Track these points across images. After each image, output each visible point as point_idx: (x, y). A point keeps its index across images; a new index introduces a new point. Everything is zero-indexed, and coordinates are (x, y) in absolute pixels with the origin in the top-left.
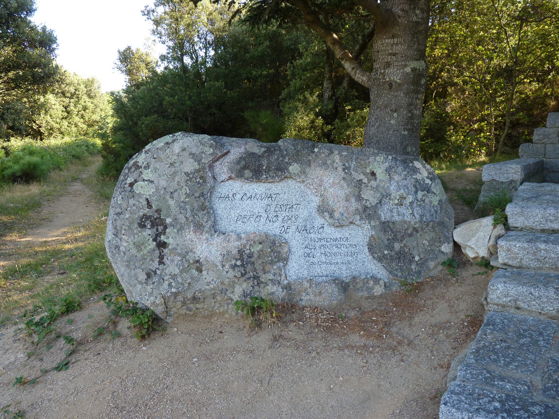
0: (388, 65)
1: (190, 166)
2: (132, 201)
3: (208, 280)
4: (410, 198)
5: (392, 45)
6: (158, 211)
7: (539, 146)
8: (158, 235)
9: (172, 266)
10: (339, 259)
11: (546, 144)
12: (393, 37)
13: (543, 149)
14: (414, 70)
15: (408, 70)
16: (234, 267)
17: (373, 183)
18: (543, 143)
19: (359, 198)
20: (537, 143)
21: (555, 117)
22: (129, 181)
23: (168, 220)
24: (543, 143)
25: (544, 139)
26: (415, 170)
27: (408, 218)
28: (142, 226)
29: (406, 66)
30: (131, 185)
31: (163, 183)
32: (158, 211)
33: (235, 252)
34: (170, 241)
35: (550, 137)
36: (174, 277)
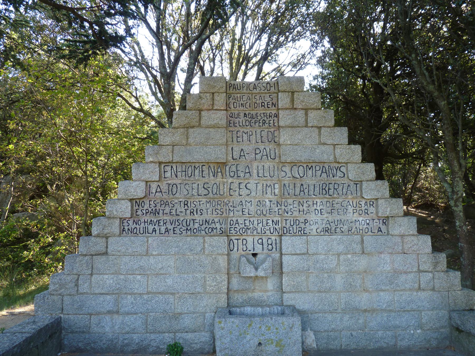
7: (55, 298)
11: (63, 296)
13: (60, 302)
18: (60, 295)
20: (53, 295)
21: (73, 261)
24: (60, 295)
25: (60, 289)
35: (67, 286)
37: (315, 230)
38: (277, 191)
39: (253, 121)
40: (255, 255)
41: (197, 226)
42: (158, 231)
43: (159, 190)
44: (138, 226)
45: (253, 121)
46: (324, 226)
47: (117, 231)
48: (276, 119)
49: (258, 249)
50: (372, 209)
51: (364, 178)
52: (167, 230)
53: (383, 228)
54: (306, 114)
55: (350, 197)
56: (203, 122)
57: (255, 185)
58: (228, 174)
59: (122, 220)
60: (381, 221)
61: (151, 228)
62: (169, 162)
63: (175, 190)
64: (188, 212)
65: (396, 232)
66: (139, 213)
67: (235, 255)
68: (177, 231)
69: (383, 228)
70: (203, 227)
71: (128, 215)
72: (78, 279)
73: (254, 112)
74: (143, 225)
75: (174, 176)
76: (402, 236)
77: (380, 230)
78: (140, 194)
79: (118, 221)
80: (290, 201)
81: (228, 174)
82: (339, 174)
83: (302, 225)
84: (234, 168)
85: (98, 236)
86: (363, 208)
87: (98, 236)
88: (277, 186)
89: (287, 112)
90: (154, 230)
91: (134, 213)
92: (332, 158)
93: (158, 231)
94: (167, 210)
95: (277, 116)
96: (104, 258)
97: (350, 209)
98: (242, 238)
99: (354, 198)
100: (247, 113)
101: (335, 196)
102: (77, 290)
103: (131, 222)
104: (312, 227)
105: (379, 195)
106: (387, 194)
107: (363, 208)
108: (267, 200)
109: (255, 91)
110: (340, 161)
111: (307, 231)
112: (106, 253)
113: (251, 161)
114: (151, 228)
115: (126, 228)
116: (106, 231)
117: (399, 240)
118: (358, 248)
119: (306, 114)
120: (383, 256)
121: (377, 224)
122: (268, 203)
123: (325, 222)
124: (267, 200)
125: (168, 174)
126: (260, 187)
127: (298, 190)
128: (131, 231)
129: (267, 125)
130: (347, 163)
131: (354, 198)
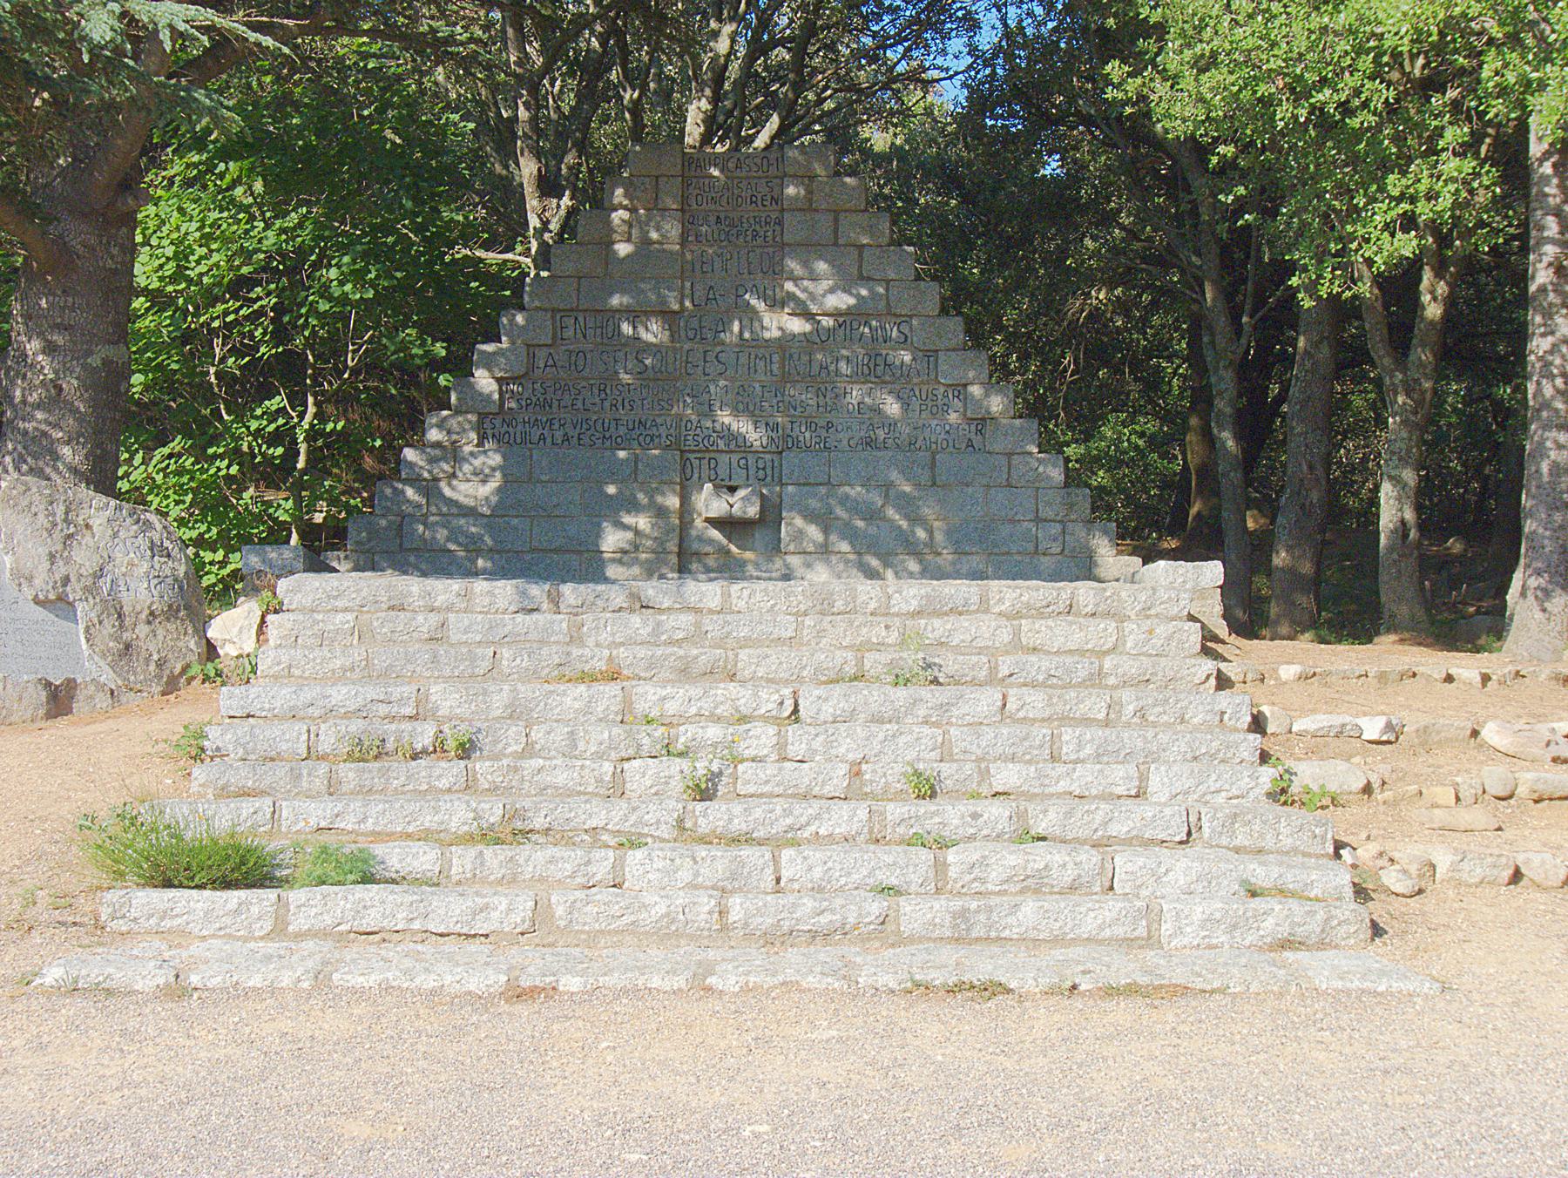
4: (146, 566)
5: (63, 309)
14: (106, 362)
15: (95, 361)
25: (369, 540)
26: (148, 525)
29: (89, 353)
37: (845, 442)
38: (775, 367)
39: (734, 231)
41: (622, 430)
42: (549, 440)
43: (550, 362)
44: (511, 430)
45: (734, 231)
46: (862, 433)
48: (778, 228)
51: (940, 345)
52: (566, 438)
53: (977, 440)
54: (836, 220)
55: (915, 380)
57: (733, 356)
58: (683, 333)
60: (973, 427)
61: (536, 433)
62: (572, 310)
63: (581, 363)
64: (607, 404)
65: (997, 448)
68: (586, 440)
70: (635, 434)
72: (401, 525)
73: (736, 215)
74: (520, 427)
75: (579, 335)
76: (1010, 455)
77: (970, 444)
81: (683, 333)
83: (824, 434)
84: (695, 323)
86: (940, 402)
88: (776, 358)
89: (799, 216)
90: (543, 438)
93: (549, 440)
94: (567, 400)
95: (780, 223)
98: (707, 456)
99: (923, 382)
100: (722, 216)
101: (887, 378)
102: (401, 545)
103: (498, 422)
104: (841, 436)
107: (940, 402)
108: (757, 385)
109: (738, 173)
110: (898, 311)
111: (831, 443)
113: (727, 312)
114: (536, 433)
115: (489, 432)
117: (1003, 461)
119: (836, 220)
120: (970, 490)
122: (758, 388)
123: (864, 427)
124: (757, 385)
125: (569, 333)
126: (743, 360)
129: (760, 241)
130: (911, 317)
131: (923, 382)
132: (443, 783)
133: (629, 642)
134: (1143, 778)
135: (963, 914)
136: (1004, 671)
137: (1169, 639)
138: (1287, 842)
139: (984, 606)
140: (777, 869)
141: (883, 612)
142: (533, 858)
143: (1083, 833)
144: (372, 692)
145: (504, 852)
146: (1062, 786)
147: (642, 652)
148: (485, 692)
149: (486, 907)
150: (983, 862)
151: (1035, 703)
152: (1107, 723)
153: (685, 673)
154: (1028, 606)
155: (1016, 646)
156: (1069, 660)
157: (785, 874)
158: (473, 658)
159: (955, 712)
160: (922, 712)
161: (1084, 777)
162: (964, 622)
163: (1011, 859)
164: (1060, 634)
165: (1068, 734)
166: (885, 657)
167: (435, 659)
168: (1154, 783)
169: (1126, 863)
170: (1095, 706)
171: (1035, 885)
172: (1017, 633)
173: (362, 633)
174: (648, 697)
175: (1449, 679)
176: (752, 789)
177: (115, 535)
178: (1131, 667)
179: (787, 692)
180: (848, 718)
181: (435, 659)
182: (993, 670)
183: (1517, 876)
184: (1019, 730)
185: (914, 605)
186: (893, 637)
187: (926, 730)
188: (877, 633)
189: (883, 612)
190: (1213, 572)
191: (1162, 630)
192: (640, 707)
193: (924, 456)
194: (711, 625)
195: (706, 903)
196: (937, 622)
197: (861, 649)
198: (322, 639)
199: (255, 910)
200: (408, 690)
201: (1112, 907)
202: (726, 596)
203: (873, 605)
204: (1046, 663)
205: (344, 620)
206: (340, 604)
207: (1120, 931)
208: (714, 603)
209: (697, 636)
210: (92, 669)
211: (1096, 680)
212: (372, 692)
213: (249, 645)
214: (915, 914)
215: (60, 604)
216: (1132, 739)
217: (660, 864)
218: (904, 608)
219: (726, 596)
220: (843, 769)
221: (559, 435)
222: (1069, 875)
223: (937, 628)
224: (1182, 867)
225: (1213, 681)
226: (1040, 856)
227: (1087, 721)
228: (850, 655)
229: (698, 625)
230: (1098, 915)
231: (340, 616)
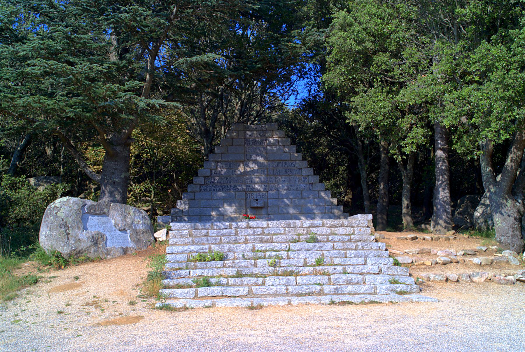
0: (113, 173)
1: (76, 207)
2: (57, 219)
3: (83, 246)
4: (141, 222)
6: (66, 222)
8: (66, 230)
9: (72, 242)
10: (121, 241)
12: (116, 161)
14: (125, 177)
15: (123, 176)
16: (91, 241)
17: (129, 216)
19: (126, 221)
22: (54, 212)
23: (70, 225)
26: (142, 213)
27: (141, 228)
28: (61, 228)
29: (121, 174)
30: (56, 213)
31: (67, 213)
32: (66, 222)
33: (91, 237)
34: (71, 232)
36: (73, 244)
38: (266, 173)
40: (257, 200)
47: (199, 190)
49: (258, 197)
50: (307, 180)
53: (311, 188)
56: (234, 143)
59: (200, 185)
61: (213, 189)
66: (207, 182)
67: (248, 200)
69: (311, 188)
71: (203, 183)
78: (208, 174)
79: (199, 186)
80: (271, 177)
82: (292, 165)
85: (191, 192)
87: (191, 192)
90: (214, 190)
91: (205, 182)
92: (289, 158)
96: (194, 201)
97: (297, 180)
105: (309, 174)
106: (313, 173)
112: (194, 199)
114: (213, 189)
116: (194, 190)
118: (300, 196)
121: (308, 186)
127: (275, 172)
128: (204, 190)
132: (219, 266)
133: (249, 235)
134: (366, 261)
135: (336, 289)
136: (330, 239)
137: (364, 231)
138: (400, 273)
139: (323, 225)
140: (296, 281)
141: (302, 227)
142: (246, 280)
143: (357, 272)
144: (200, 247)
145: (240, 279)
146: (349, 263)
147: (252, 237)
148: (223, 246)
149: (239, 290)
150: (338, 278)
151: (340, 245)
152: (355, 249)
153: (262, 241)
154: (333, 225)
155: (332, 234)
156: (344, 236)
157: (298, 282)
158: (216, 239)
159: (323, 248)
160: (316, 248)
161: (353, 261)
162: (320, 228)
163: (344, 277)
164: (341, 231)
165: (348, 252)
166: (304, 237)
167: (208, 240)
168: (368, 262)
169: (367, 277)
170: (353, 245)
171: (349, 282)
172: (331, 231)
173: (191, 235)
174: (258, 246)
175: (424, 239)
176: (284, 265)
177: (135, 215)
178: (357, 237)
179: (287, 244)
180: (301, 249)
181: (208, 240)
182: (328, 239)
183: (447, 280)
184: (338, 251)
185: (308, 225)
186: (305, 232)
187: (318, 252)
188: (301, 232)
189: (302, 227)
190: (370, 216)
191: (363, 229)
192: (257, 249)
193: (300, 192)
194: (266, 231)
195: (284, 288)
196: (314, 229)
197: (299, 235)
198: (182, 236)
199: (191, 292)
200: (207, 246)
201: (367, 287)
202: (268, 224)
203: (299, 225)
204: (339, 237)
205: (186, 232)
206: (184, 228)
207: (368, 292)
208: (265, 226)
209: (263, 233)
210: (131, 244)
211: (350, 240)
212: (200, 247)
213: (164, 238)
214: (327, 289)
215: (124, 231)
216: (362, 252)
217: (272, 280)
218: (306, 226)
219: (268, 224)
220: (303, 260)
221: (218, 189)
222: (356, 281)
223: (314, 230)
224: (380, 278)
225: (375, 240)
226: (350, 276)
227: (352, 249)
228: (297, 236)
229: (263, 231)
230: (362, 288)
231: (185, 231)
